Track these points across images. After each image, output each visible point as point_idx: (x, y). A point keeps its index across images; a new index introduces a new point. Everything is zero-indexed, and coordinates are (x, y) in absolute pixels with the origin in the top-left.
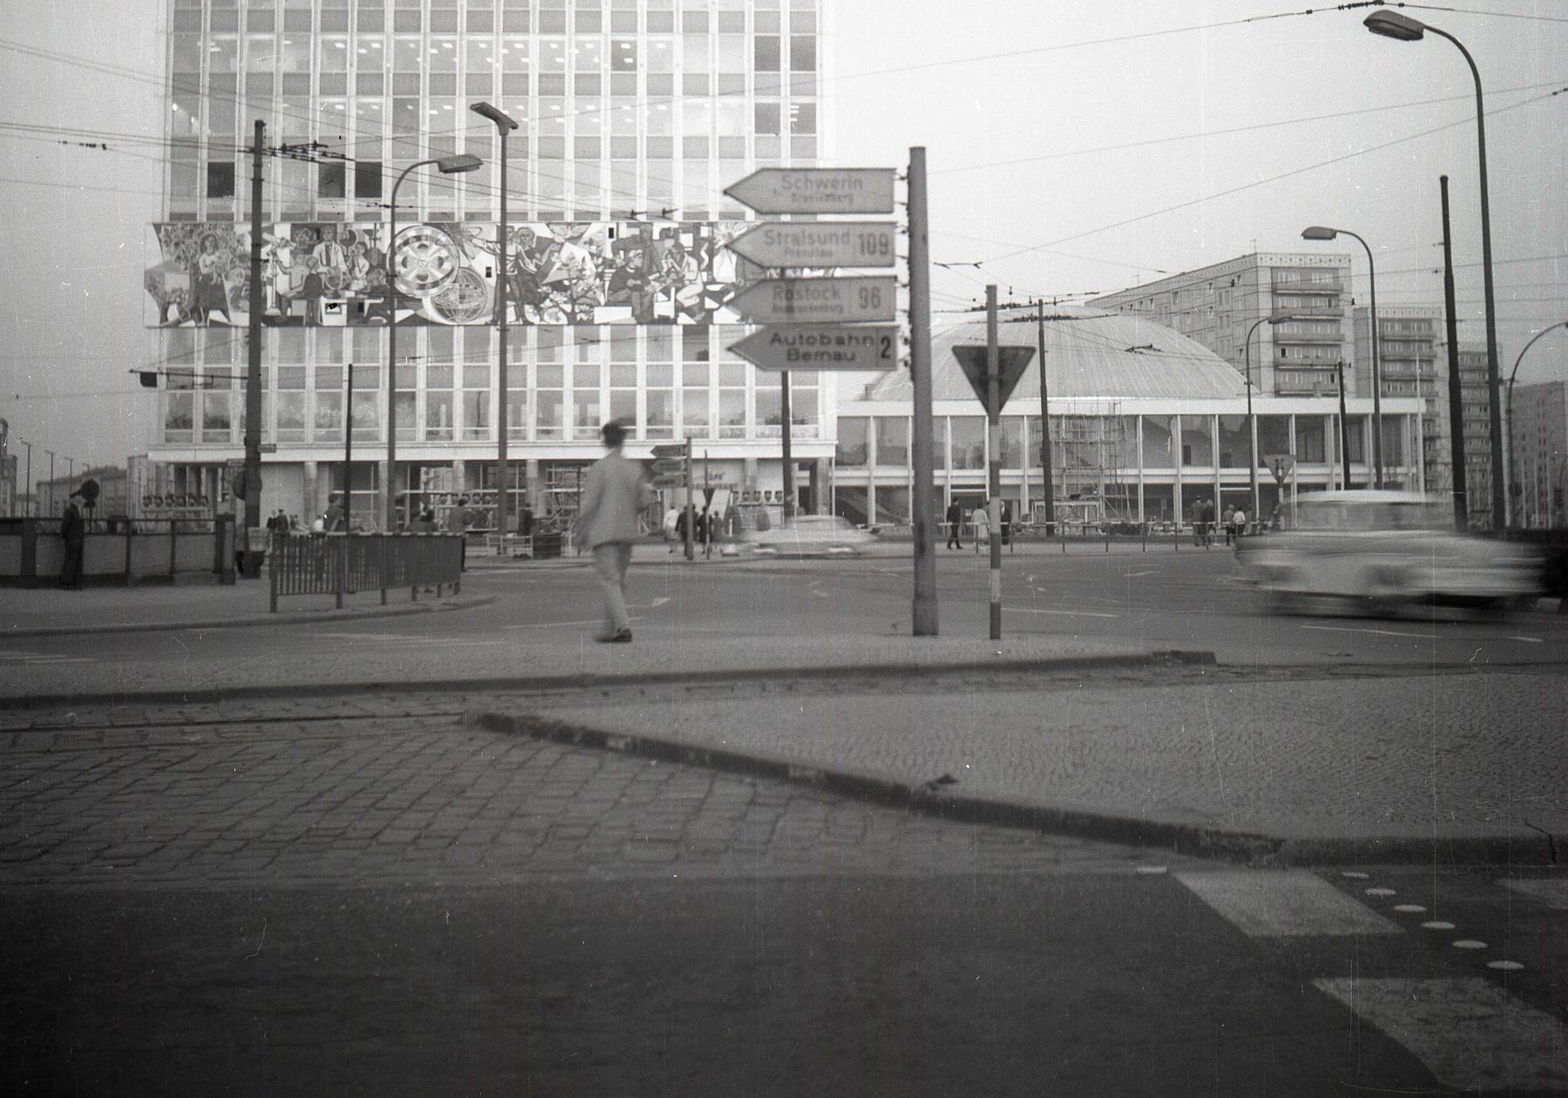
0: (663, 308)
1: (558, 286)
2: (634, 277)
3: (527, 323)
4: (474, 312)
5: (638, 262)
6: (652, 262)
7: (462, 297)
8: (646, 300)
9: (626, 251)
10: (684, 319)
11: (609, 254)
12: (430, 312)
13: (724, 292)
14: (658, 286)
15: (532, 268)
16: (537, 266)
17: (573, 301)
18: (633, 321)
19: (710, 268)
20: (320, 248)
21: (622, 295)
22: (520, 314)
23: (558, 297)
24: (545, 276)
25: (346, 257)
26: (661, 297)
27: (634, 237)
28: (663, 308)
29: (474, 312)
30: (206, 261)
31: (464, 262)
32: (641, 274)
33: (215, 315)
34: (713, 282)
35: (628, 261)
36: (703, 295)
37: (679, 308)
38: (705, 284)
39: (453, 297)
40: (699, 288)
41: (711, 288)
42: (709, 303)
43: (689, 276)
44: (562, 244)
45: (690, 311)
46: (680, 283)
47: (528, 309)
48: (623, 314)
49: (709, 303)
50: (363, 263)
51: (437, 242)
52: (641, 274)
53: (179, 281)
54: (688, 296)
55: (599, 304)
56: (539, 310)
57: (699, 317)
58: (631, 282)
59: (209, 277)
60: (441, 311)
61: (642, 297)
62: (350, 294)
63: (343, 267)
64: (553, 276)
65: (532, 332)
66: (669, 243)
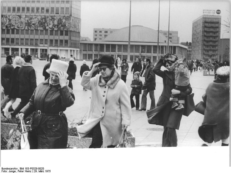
1: (33, 24)
2: (43, 23)
3: (29, 29)
4: (22, 28)
5: (44, 21)
6: (46, 21)
7: (21, 25)
8: (45, 27)
9: (42, 19)
10: (50, 29)
11: (40, 20)
12: (16, 27)
13: (56, 26)
14: (46, 25)
15: (30, 21)
16: (31, 21)
17: (35, 26)
18: (43, 29)
19: (54, 22)
21: (42, 26)
22: (28, 28)
23: (33, 26)
24: (32, 22)
25: (6, 19)
26: (47, 26)
27: (43, 18)
29: (22, 28)
31: (21, 20)
32: (44, 23)
34: (54, 24)
35: (43, 21)
36: (53, 26)
38: (53, 24)
39: (19, 25)
40: (52, 25)
41: (54, 25)
42: (53, 27)
44: (34, 19)
45: (51, 28)
47: (29, 27)
48: (42, 28)
49: (53, 27)
50: (8, 20)
51: (18, 18)
52: (44, 23)
55: (38, 27)
56: (30, 28)
57: (52, 29)
58: (43, 24)
60: (18, 27)
61: (44, 26)
62: (6, 25)
63: (5, 21)
64: (33, 23)
65: (30, 31)
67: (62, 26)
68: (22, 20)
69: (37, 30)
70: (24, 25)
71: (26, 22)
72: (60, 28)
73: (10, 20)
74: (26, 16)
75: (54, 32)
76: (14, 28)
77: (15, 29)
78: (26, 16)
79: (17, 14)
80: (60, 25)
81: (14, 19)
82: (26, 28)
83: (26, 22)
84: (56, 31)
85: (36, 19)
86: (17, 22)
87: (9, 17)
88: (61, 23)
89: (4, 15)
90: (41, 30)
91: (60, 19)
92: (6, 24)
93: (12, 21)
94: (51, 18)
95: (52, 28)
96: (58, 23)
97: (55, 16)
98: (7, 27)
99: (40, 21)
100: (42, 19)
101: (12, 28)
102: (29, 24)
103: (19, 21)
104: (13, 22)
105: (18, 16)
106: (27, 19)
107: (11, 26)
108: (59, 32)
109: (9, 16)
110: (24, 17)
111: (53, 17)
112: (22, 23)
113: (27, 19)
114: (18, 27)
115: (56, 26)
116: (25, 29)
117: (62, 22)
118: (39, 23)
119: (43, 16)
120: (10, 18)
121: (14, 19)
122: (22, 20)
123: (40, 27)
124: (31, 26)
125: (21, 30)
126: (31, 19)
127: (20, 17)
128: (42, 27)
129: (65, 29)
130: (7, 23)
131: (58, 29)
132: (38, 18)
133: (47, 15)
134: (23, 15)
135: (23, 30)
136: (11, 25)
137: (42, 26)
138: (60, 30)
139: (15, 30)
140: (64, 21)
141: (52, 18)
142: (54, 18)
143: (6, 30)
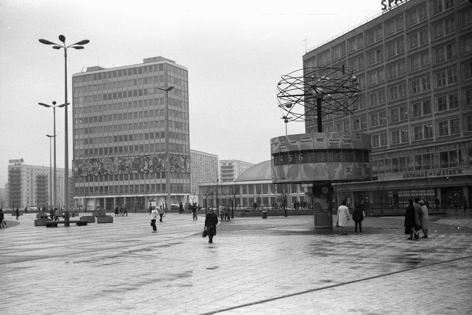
0: (142, 170)
1: (127, 167)
3: (123, 174)
4: (115, 172)
10: (145, 172)
11: (134, 161)
12: (109, 173)
13: (151, 167)
17: (129, 170)
19: (148, 163)
20: (94, 163)
21: (136, 168)
22: (122, 173)
23: (127, 169)
28: (142, 170)
29: (115, 172)
30: (80, 165)
33: (81, 174)
36: (148, 167)
37: (144, 170)
39: (112, 170)
40: (147, 167)
42: (149, 169)
43: (146, 164)
45: (146, 171)
46: (144, 166)
48: (136, 172)
50: (100, 165)
52: (139, 165)
53: (76, 169)
54: (145, 168)
59: (80, 168)
60: (111, 172)
64: (127, 165)
66: (143, 159)
67: (158, 167)
68: (116, 163)
69: (131, 174)
70: (117, 168)
71: (120, 165)
72: (156, 169)
73: (102, 165)
74: (119, 157)
75: (150, 174)
76: (107, 174)
77: (109, 174)
78: (119, 157)
79: (110, 157)
80: (156, 166)
81: (107, 162)
82: (120, 173)
83: (120, 165)
84: (152, 173)
85: (130, 161)
86: (110, 166)
87: (102, 161)
88: (157, 163)
89: (96, 159)
90: (135, 174)
91: (155, 157)
92: (98, 169)
93: (104, 166)
94: (145, 158)
95: (147, 169)
96: (153, 164)
97: (149, 155)
98: (99, 173)
99: (134, 163)
100: (136, 160)
101: (105, 173)
102: (122, 168)
103: (112, 164)
104: (105, 166)
105: (110, 158)
106: (120, 161)
107: (103, 172)
108: (155, 174)
109: (101, 160)
110: (117, 159)
111: (148, 157)
112: (115, 166)
113: (120, 161)
114: (111, 172)
115: (151, 167)
116: (118, 173)
117: (158, 161)
118: (133, 165)
119: (137, 156)
120: (102, 162)
121: (107, 162)
122: (116, 163)
123: (134, 170)
124: (125, 169)
125: (115, 175)
126: (125, 160)
127: (113, 159)
128: (137, 169)
129: (161, 170)
130: (99, 169)
131: (154, 171)
132: (131, 159)
133: (142, 154)
134: (116, 156)
135: (117, 175)
136: (103, 170)
137: (136, 168)
138: (156, 171)
139: (109, 176)
140: (160, 160)
141: (147, 158)
142: (149, 158)
143: (99, 177)
